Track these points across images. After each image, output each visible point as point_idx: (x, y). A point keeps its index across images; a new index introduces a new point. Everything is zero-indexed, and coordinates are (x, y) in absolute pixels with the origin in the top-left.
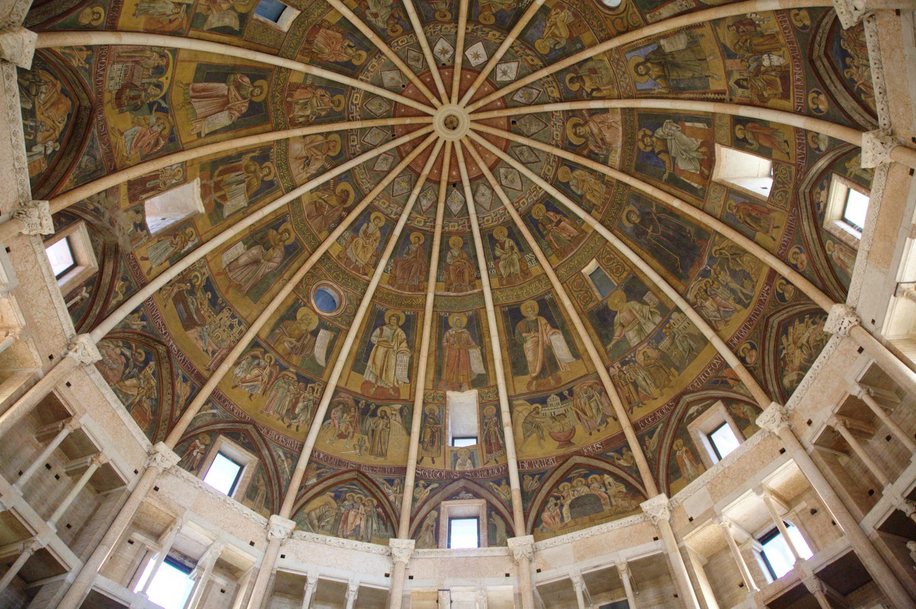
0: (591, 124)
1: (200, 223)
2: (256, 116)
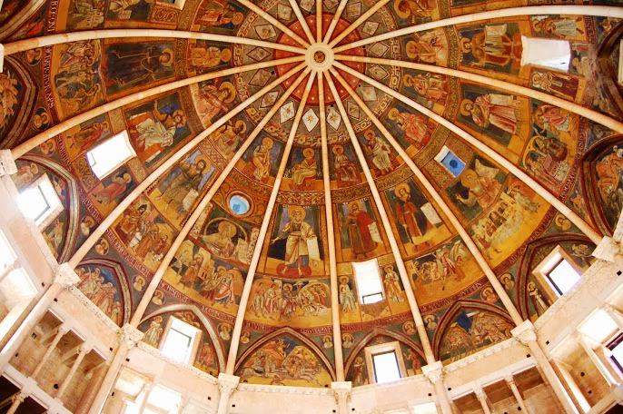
0: (218, 103)
1: (527, 29)
2: (471, 92)
